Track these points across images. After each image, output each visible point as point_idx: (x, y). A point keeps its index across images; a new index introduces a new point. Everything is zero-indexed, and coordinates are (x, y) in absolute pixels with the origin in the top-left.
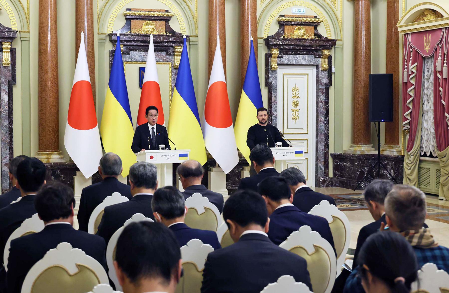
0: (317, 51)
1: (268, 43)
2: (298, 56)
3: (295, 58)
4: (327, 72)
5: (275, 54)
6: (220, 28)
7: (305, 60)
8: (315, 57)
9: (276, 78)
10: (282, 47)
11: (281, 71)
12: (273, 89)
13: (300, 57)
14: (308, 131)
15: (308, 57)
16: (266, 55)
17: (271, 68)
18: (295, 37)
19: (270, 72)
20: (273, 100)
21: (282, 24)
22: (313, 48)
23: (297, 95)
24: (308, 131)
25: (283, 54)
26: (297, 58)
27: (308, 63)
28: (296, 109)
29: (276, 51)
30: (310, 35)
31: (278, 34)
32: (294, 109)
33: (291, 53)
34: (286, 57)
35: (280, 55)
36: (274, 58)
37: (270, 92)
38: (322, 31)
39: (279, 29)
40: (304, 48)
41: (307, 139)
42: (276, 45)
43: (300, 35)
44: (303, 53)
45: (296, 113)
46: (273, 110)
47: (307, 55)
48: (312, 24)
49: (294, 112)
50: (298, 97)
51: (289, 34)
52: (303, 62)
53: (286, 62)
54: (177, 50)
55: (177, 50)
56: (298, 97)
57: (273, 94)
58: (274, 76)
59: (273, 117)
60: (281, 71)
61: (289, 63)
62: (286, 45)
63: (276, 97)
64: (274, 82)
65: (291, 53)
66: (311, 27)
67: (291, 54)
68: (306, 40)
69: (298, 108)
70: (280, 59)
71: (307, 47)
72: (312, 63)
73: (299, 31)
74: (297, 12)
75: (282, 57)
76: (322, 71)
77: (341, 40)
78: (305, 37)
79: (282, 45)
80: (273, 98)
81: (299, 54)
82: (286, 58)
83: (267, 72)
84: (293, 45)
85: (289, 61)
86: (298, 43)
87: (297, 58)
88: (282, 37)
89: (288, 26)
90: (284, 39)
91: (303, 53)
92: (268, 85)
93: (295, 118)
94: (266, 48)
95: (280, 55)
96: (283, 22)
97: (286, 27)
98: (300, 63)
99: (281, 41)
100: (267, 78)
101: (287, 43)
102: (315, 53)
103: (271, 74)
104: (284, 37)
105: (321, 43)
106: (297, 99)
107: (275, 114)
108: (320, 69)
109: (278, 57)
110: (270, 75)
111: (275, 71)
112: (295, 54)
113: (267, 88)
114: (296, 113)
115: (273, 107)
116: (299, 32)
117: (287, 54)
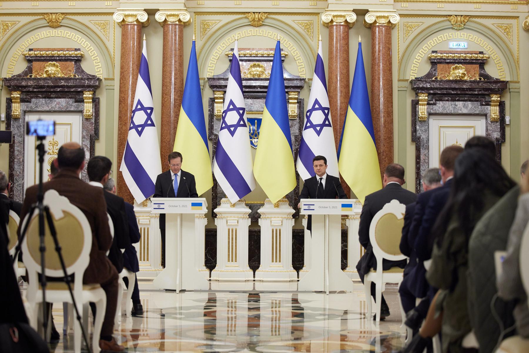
0: (483, 95)
1: (417, 86)
2: (457, 103)
3: (453, 106)
4: (498, 124)
5: (422, 100)
6: (340, 68)
7: (467, 108)
8: (482, 105)
9: (427, 130)
10: (432, 92)
11: (434, 123)
12: (422, 144)
13: (460, 104)
15: (472, 104)
16: (412, 101)
17: (419, 117)
18: (451, 78)
20: (422, 159)
21: (434, 63)
22: (476, 93)
25: (436, 100)
26: (457, 106)
27: (471, 112)
30: (474, 76)
31: (429, 75)
33: (446, 98)
34: (440, 104)
35: (432, 102)
36: (423, 105)
37: (418, 150)
38: (494, 71)
39: (431, 68)
40: (463, 92)
42: (423, 89)
43: (457, 76)
44: (463, 99)
47: (470, 101)
48: (474, 61)
51: (443, 75)
52: (465, 111)
53: (440, 111)
57: (422, 151)
58: (423, 128)
60: (434, 123)
61: (445, 112)
62: (437, 89)
63: (427, 156)
64: (423, 136)
65: (446, 98)
66: (474, 66)
67: (448, 100)
68: (466, 81)
70: (431, 107)
71: (467, 91)
72: (477, 112)
73: (457, 71)
74: (455, 47)
75: (435, 104)
76: (492, 122)
77: (516, 82)
78: (466, 78)
79: (431, 89)
80: (422, 157)
81: (458, 100)
82: (440, 106)
84: (446, 89)
86: (453, 86)
87: (457, 106)
88: (433, 79)
89: (442, 65)
90: (436, 81)
91: (463, 99)
92: (416, 139)
94: (414, 93)
95: (432, 102)
96: (434, 59)
97: (440, 66)
98: (460, 112)
99: (429, 83)
100: (414, 131)
101: (437, 85)
102: (480, 98)
103: (419, 126)
104: (436, 78)
105: (485, 86)
108: (489, 119)
109: (428, 104)
110: (418, 127)
111: (424, 122)
112: (453, 100)
113: (415, 143)
115: (421, 168)
116: (458, 72)
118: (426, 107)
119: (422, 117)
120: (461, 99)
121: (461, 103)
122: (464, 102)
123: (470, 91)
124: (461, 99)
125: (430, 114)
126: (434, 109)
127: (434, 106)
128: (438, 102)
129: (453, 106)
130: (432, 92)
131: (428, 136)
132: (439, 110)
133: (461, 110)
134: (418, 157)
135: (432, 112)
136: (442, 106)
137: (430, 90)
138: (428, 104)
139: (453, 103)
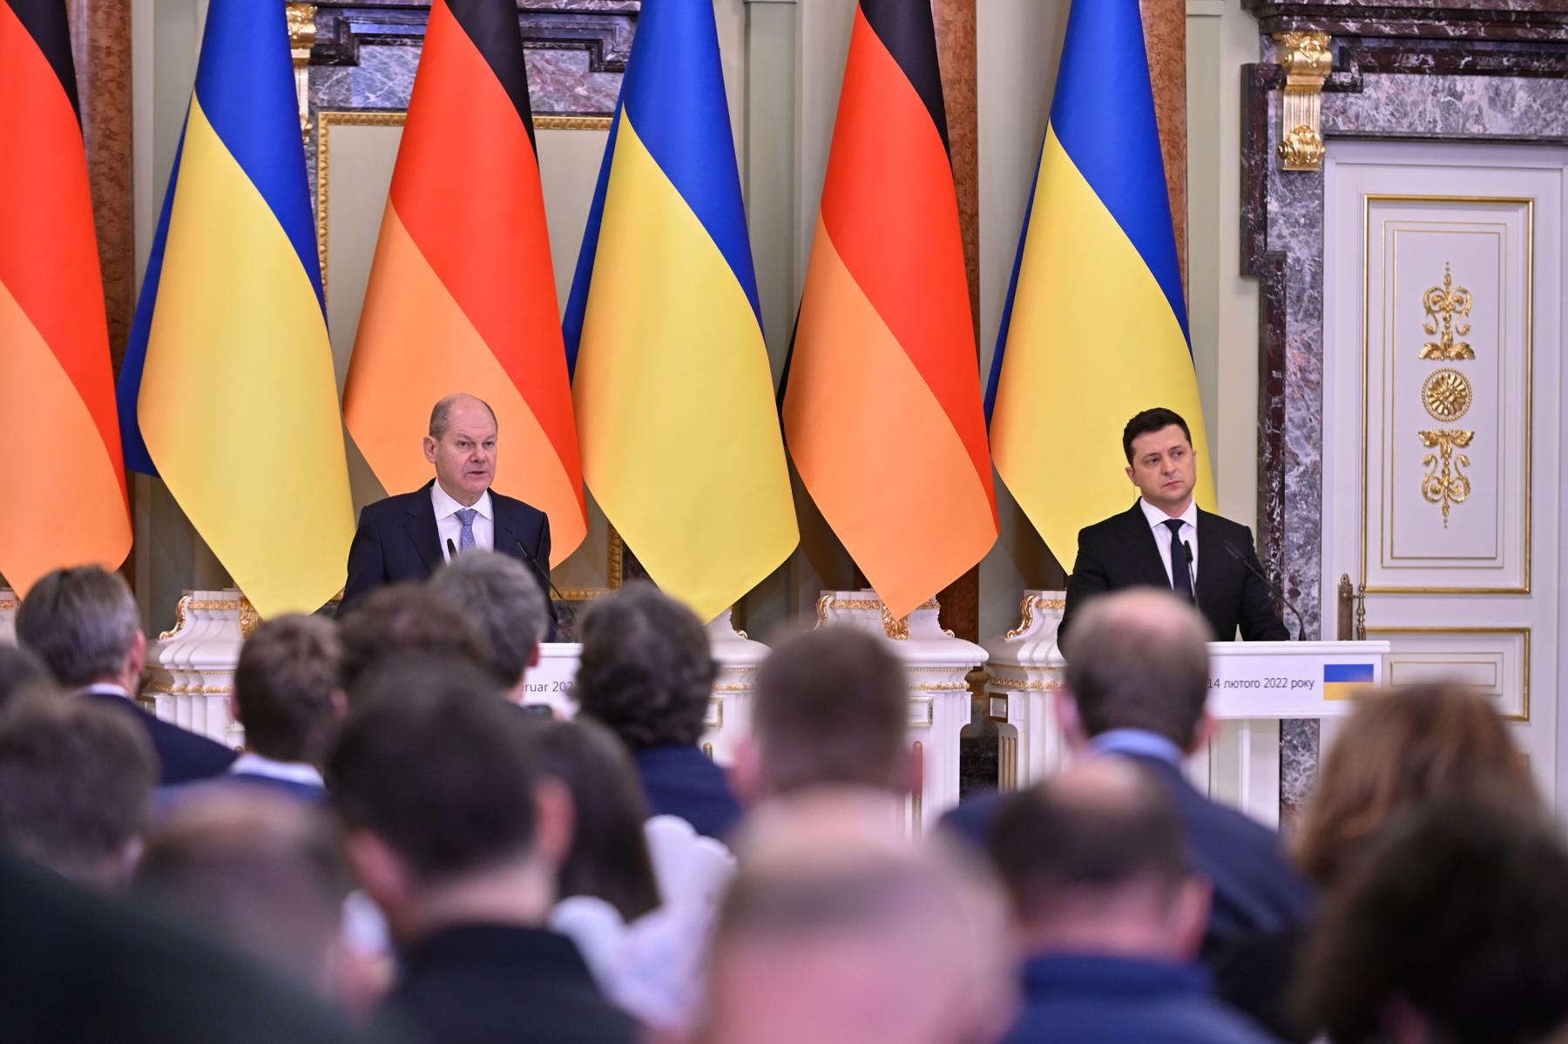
2: (1461, 83)
3: (1444, 98)
5: (1304, 68)
7: (1505, 108)
9: (1314, 222)
10: (1352, 26)
11: (1347, 182)
12: (1292, 293)
13: (1474, 88)
14: (1528, 574)
15: (1532, 91)
16: (1248, 72)
17: (1283, 156)
19: (1276, 184)
23: (1458, 340)
24: (1528, 574)
25: (1364, 69)
26: (1459, 97)
27: (1528, 131)
28: (1447, 428)
29: (1310, 51)
32: (1435, 427)
33: (1413, 60)
34: (1381, 86)
35: (1344, 78)
36: (1303, 91)
37: (1272, 317)
41: (1524, 631)
44: (1493, 62)
45: (1446, 455)
46: (1292, 435)
47: (1525, 73)
49: (1436, 451)
50: (1468, 352)
52: (1498, 125)
53: (1382, 120)
54: (1298, 57)
55: (1298, 57)
56: (1468, 352)
57: (1293, 326)
58: (1298, 211)
59: (1291, 479)
61: (1403, 129)
63: (1313, 349)
64: (1298, 252)
65: (1413, 60)
69: (1461, 425)
70: (1338, 100)
75: (1356, 87)
80: (1293, 357)
81: (1471, 70)
82: (1382, 97)
83: (1253, 186)
85: (1400, 110)
87: (1459, 97)
91: (1493, 62)
92: (1260, 263)
93: (1440, 493)
95: (1344, 78)
98: (1475, 129)
100: (1254, 226)
103: (1281, 200)
106: (1457, 365)
107: (1307, 457)
109: (1330, 87)
110: (1273, 206)
111: (1306, 176)
112: (1446, 67)
114: (1446, 455)
115: (1290, 412)
117: (1387, 68)
118: (1316, 102)
119: (1301, 156)
120: (1483, 63)
121: (1479, 82)
122: (1495, 81)
123: (1535, 24)
124: (1483, 63)
125: (1330, 136)
126: (1352, 113)
127: (1352, 98)
128: (1372, 77)
129: (1444, 98)
130: (1352, 26)
131: (1321, 254)
132: (1373, 121)
133: (1478, 119)
134: (1271, 360)
135: (1342, 126)
136: (1390, 99)
137: (1344, 18)
138: (1330, 87)
139: (1441, 82)
